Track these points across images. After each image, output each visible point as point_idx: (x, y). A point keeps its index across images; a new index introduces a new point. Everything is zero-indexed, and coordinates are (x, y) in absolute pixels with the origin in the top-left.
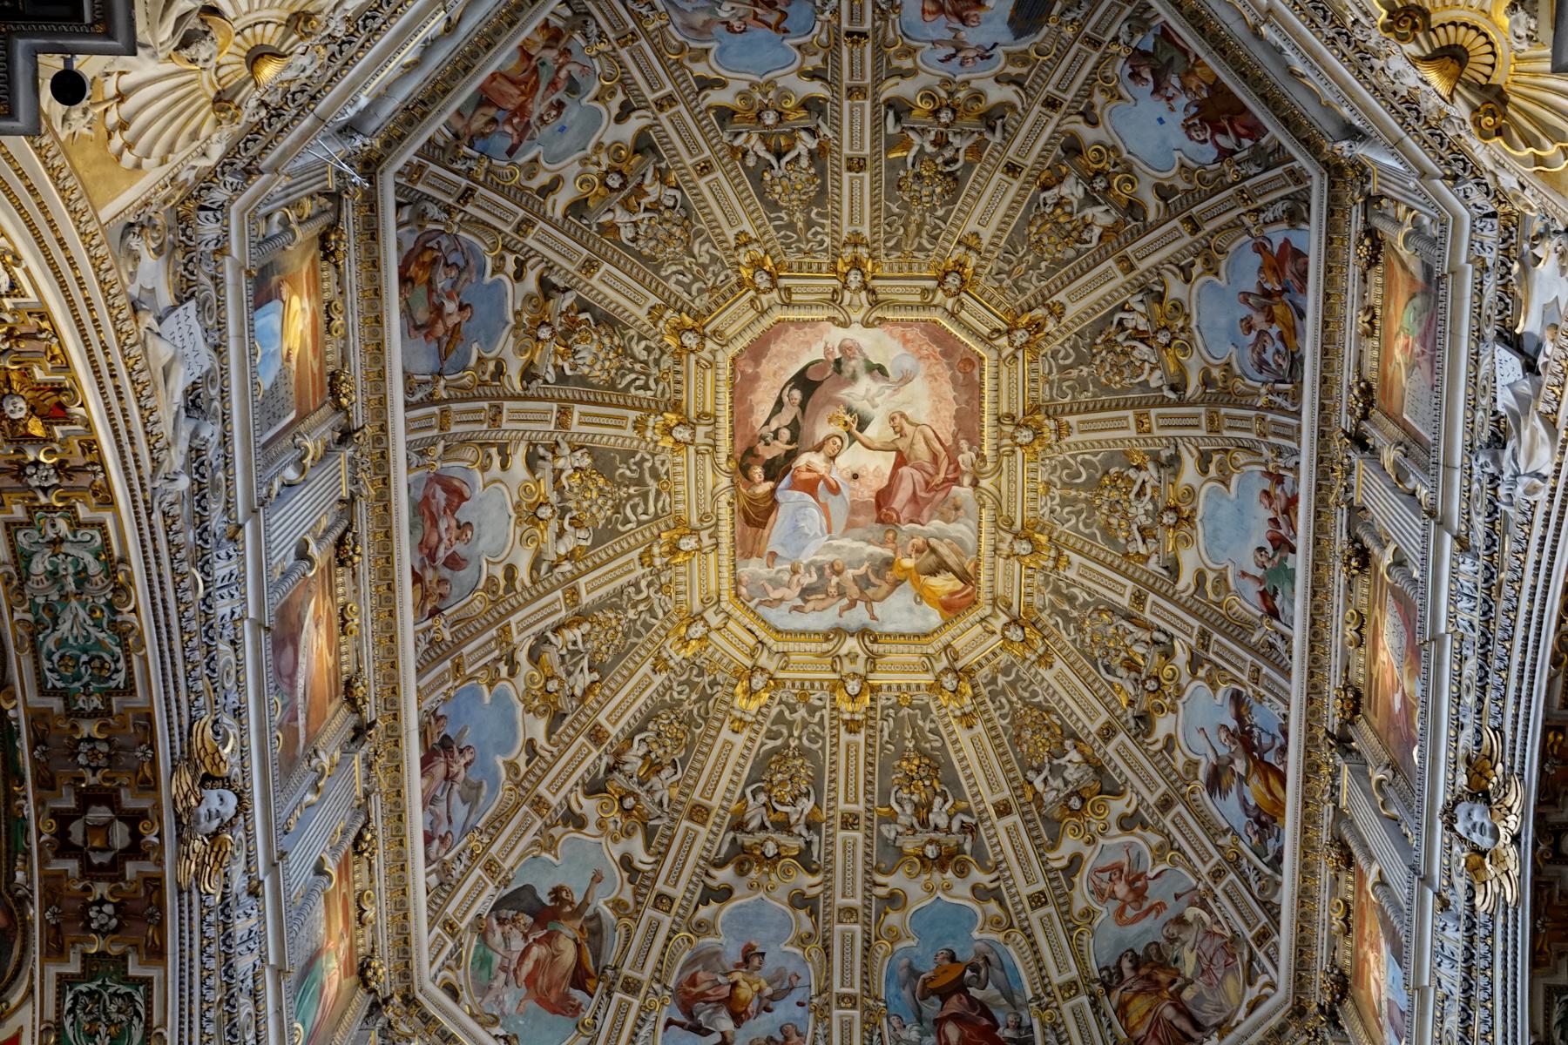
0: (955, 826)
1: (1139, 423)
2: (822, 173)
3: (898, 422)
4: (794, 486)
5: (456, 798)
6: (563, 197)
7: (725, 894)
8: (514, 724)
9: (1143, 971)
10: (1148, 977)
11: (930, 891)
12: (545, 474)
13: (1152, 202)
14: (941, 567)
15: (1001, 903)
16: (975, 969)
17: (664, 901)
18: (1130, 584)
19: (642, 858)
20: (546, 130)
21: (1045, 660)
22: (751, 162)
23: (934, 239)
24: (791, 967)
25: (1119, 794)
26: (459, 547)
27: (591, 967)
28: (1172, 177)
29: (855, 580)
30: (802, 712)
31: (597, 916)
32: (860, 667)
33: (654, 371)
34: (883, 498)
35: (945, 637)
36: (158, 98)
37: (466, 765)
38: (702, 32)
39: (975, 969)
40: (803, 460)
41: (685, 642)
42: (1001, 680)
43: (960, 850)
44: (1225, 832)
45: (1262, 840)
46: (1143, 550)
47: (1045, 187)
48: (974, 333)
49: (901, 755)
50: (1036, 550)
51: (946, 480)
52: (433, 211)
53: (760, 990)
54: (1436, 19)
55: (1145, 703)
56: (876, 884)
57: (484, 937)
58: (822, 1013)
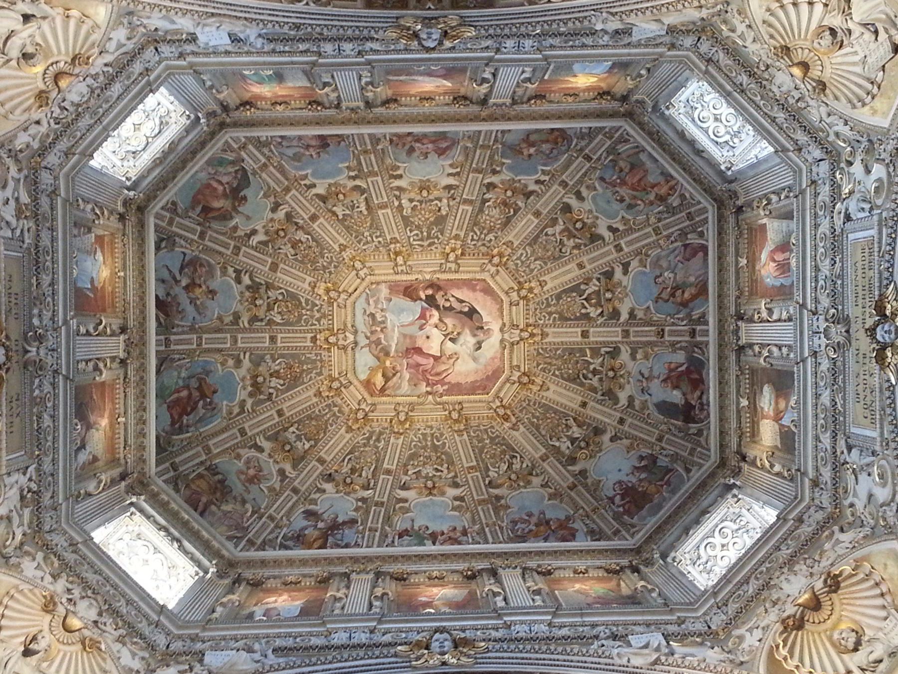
0: (271, 391)
1: (472, 468)
2: (576, 319)
3: (455, 356)
4: (424, 310)
5: (297, 150)
6: (573, 202)
7: (238, 281)
8: (324, 178)
9: (219, 486)
10: (216, 488)
11: (243, 379)
12: (445, 194)
13: (577, 468)
14: (387, 379)
15: (238, 414)
16: (211, 403)
17: (237, 249)
18: (394, 467)
19: (254, 241)
20: (610, 194)
21: (349, 429)
22: (583, 287)
23: (544, 370)
24: (209, 313)
25: (294, 467)
26: (417, 153)
27: (210, 215)
28: (592, 476)
29: (379, 339)
30: (317, 315)
31: (232, 218)
32: (341, 342)
33: (480, 243)
34: (419, 351)
35: (356, 382)
36: (799, 21)
37: (311, 155)
38: (656, 263)
39: (211, 403)
40: (435, 313)
41: (353, 259)
42: (336, 409)
43: (261, 393)
44: (288, 520)
45: (291, 539)
46: (410, 473)
47: (575, 419)
48: (500, 390)
49: (301, 363)
50: (402, 423)
51: (428, 379)
52: (583, 143)
53: (198, 299)
54: (834, 595)
55: (339, 478)
56: (245, 353)
57: (233, 163)
58: (192, 329)
